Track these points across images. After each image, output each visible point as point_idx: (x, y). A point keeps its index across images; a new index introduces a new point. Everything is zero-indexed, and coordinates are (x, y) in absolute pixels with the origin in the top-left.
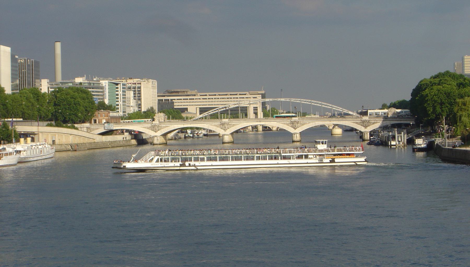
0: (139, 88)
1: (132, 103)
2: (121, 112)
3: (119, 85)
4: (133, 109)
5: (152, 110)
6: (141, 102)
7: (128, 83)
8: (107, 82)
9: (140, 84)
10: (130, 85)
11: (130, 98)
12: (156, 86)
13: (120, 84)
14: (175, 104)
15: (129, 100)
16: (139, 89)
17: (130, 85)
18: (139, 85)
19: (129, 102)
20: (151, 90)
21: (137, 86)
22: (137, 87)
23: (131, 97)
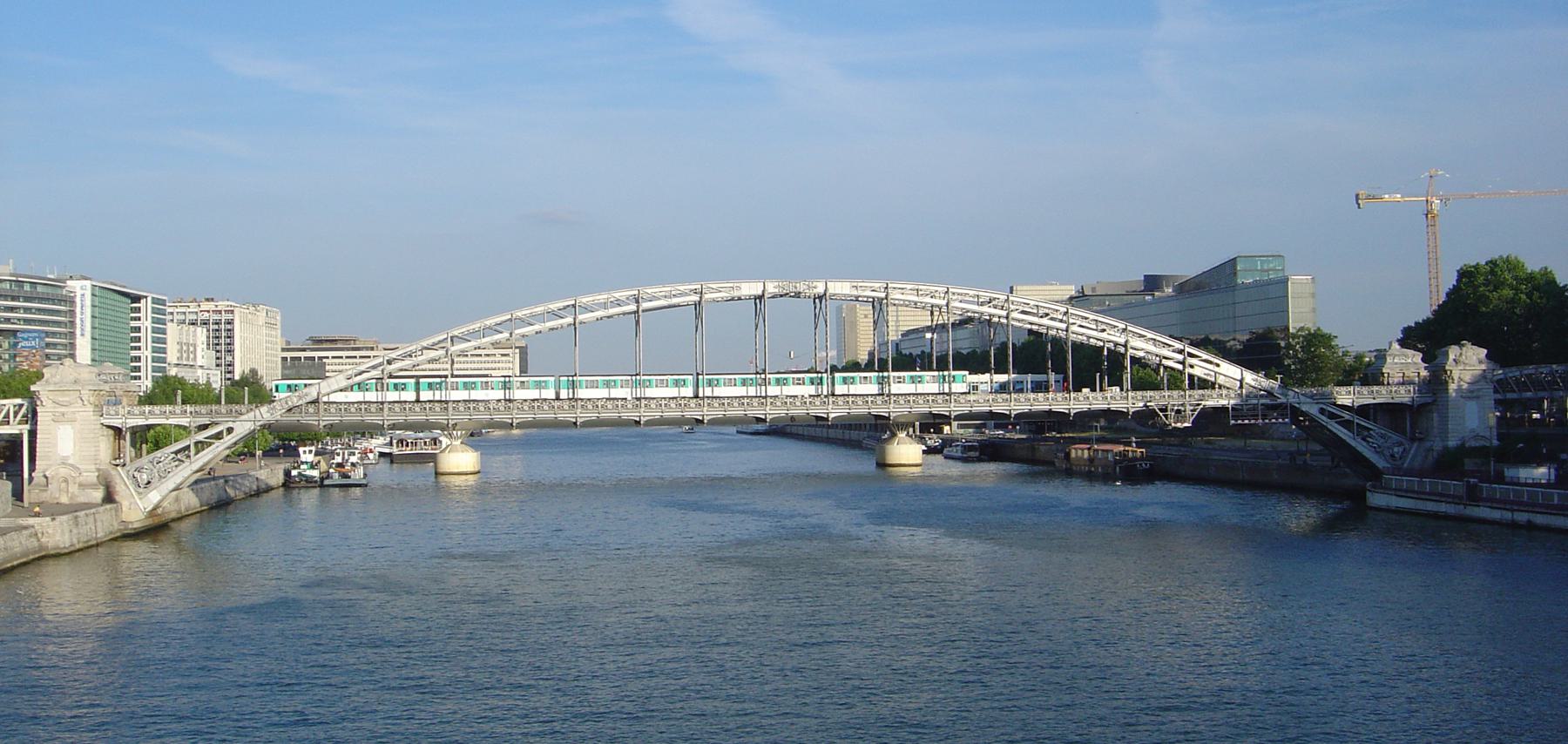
0: (229, 323)
1: (203, 357)
2: (147, 379)
3: (143, 301)
4: (205, 375)
5: (253, 377)
6: (233, 358)
7: (201, 311)
8: (89, 287)
9: (232, 312)
10: (208, 315)
11: (195, 346)
12: (279, 324)
13: (146, 297)
14: (327, 368)
15: (191, 349)
16: (229, 327)
17: (207, 314)
18: (230, 316)
19: (191, 356)
20: (264, 331)
21: (224, 317)
22: (223, 321)
23: (199, 343)
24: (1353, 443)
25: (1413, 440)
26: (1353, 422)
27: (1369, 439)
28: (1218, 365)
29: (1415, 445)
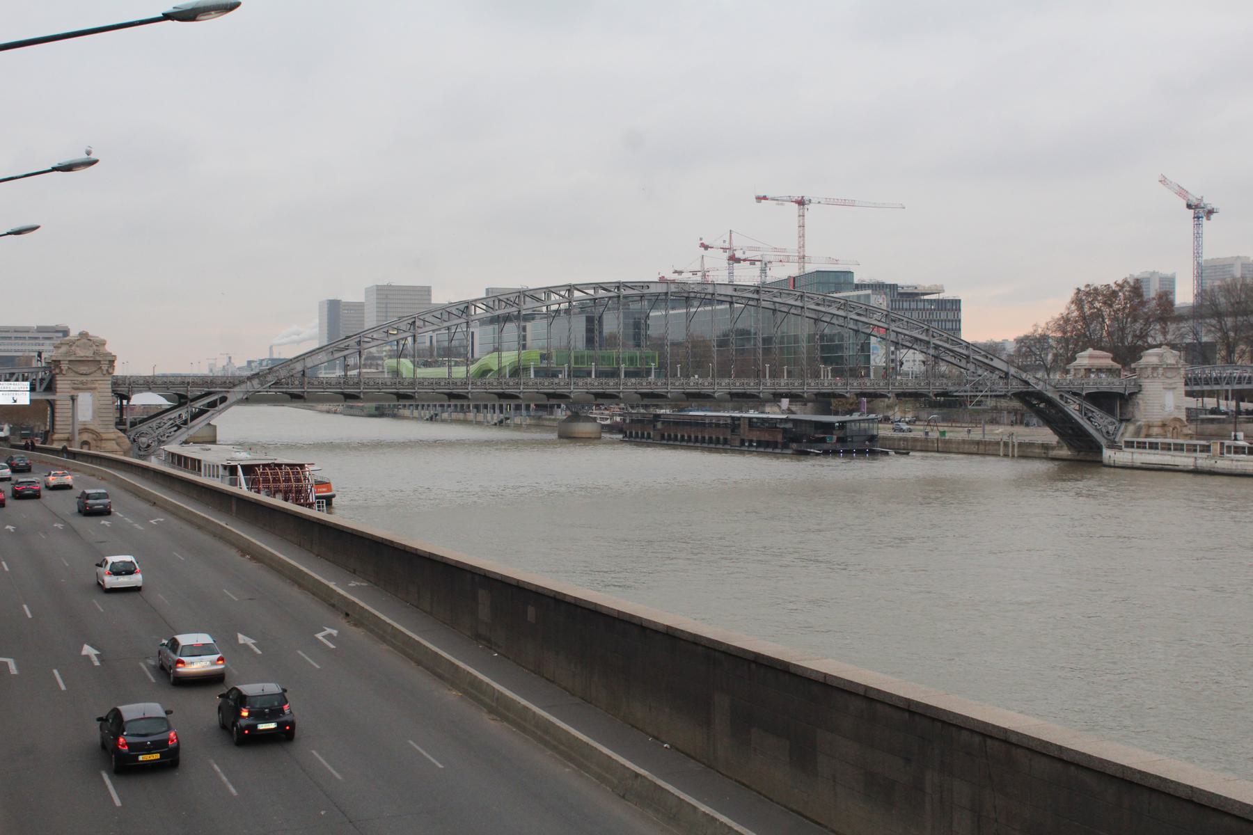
25: (1121, 421)
27: (1091, 419)
28: (992, 360)
29: (1124, 424)
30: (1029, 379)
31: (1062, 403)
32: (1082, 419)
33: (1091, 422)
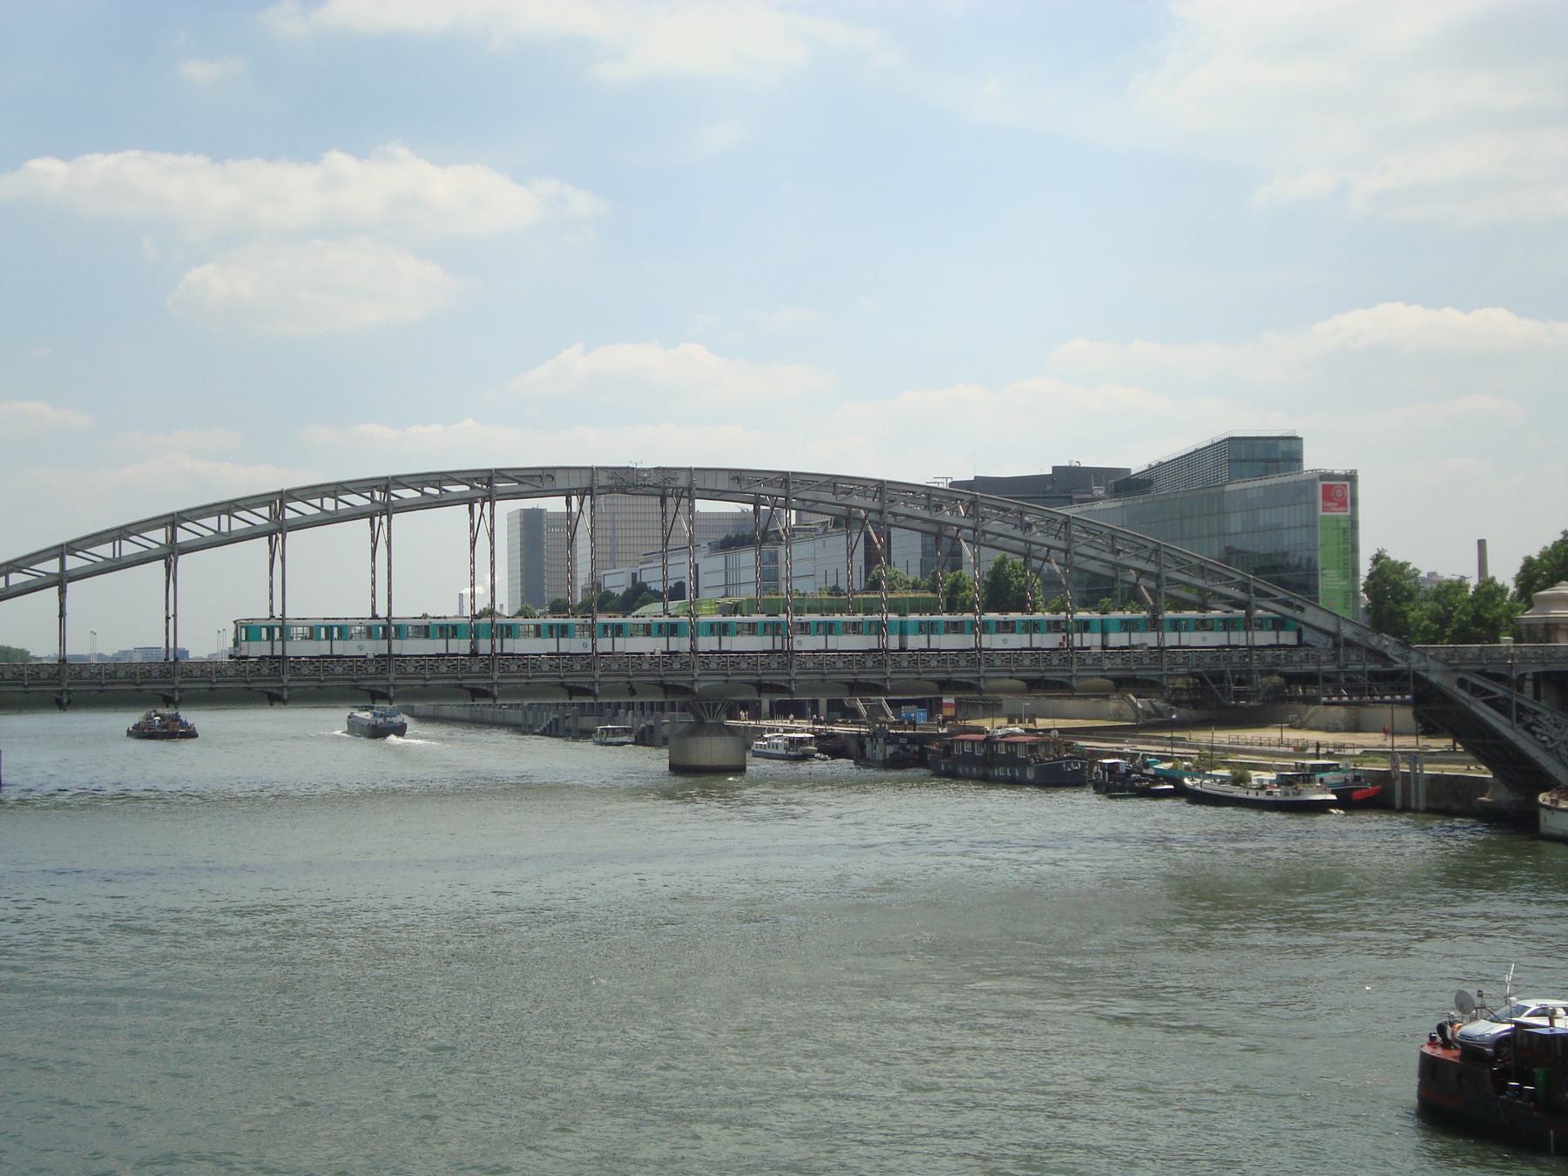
24: (1509, 734)
26: (1509, 701)
27: (1534, 728)
28: (1302, 609)
30: (1386, 646)
31: (1464, 694)
32: (1512, 727)
33: (1534, 733)
